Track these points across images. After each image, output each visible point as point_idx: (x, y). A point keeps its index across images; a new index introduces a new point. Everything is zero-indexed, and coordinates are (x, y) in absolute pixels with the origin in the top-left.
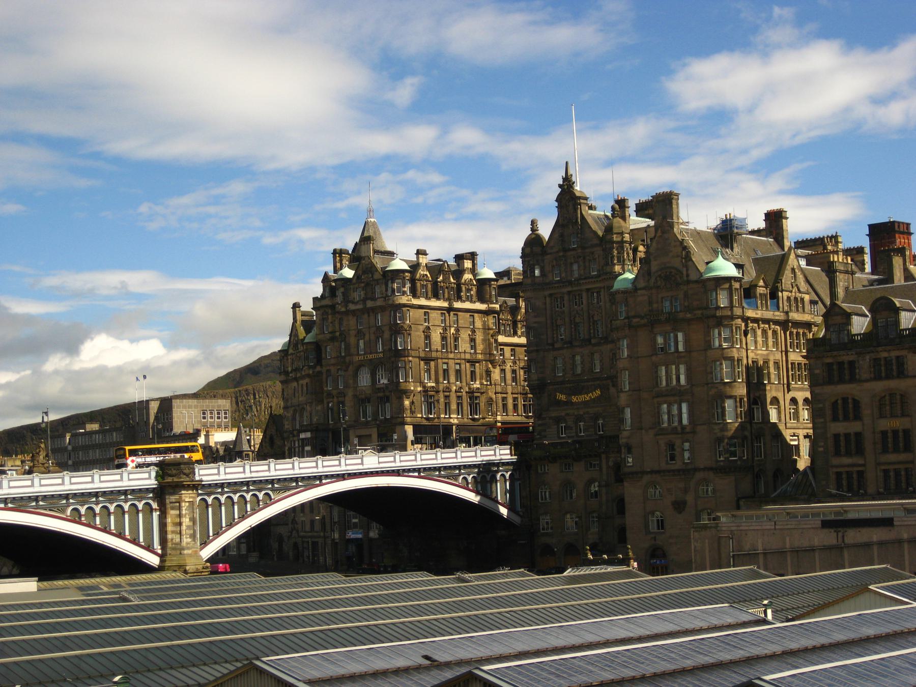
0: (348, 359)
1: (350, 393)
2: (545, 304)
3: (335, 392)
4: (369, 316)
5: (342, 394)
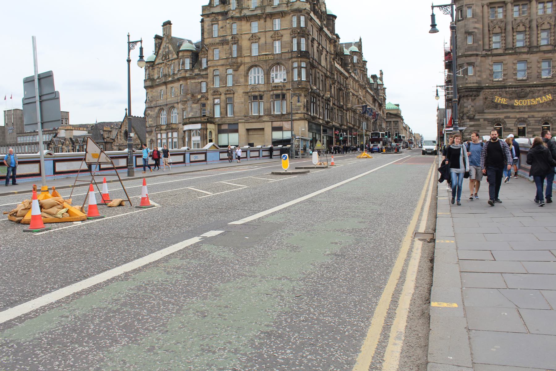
0: (239, 60)
1: (240, 91)
2: (483, 12)
3: (222, 90)
4: (265, 21)
5: (230, 92)
